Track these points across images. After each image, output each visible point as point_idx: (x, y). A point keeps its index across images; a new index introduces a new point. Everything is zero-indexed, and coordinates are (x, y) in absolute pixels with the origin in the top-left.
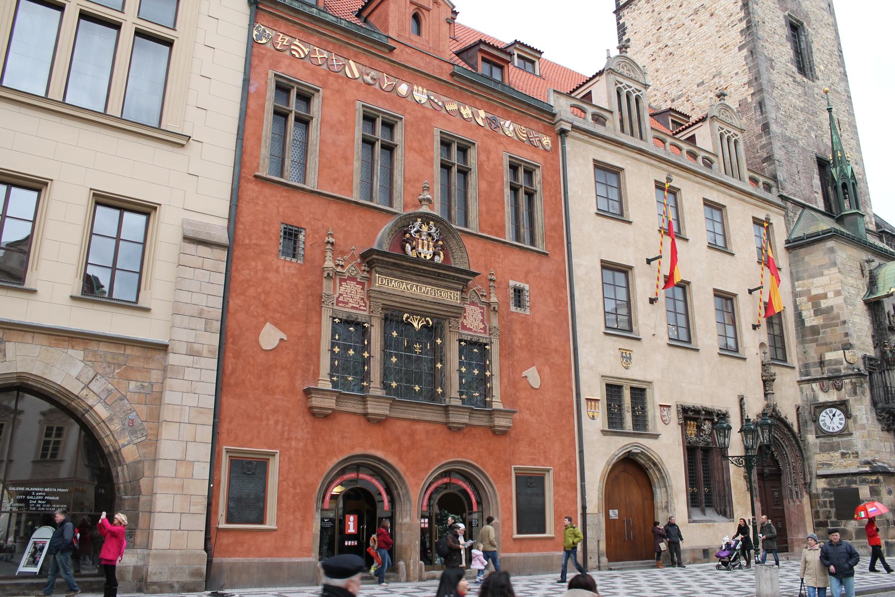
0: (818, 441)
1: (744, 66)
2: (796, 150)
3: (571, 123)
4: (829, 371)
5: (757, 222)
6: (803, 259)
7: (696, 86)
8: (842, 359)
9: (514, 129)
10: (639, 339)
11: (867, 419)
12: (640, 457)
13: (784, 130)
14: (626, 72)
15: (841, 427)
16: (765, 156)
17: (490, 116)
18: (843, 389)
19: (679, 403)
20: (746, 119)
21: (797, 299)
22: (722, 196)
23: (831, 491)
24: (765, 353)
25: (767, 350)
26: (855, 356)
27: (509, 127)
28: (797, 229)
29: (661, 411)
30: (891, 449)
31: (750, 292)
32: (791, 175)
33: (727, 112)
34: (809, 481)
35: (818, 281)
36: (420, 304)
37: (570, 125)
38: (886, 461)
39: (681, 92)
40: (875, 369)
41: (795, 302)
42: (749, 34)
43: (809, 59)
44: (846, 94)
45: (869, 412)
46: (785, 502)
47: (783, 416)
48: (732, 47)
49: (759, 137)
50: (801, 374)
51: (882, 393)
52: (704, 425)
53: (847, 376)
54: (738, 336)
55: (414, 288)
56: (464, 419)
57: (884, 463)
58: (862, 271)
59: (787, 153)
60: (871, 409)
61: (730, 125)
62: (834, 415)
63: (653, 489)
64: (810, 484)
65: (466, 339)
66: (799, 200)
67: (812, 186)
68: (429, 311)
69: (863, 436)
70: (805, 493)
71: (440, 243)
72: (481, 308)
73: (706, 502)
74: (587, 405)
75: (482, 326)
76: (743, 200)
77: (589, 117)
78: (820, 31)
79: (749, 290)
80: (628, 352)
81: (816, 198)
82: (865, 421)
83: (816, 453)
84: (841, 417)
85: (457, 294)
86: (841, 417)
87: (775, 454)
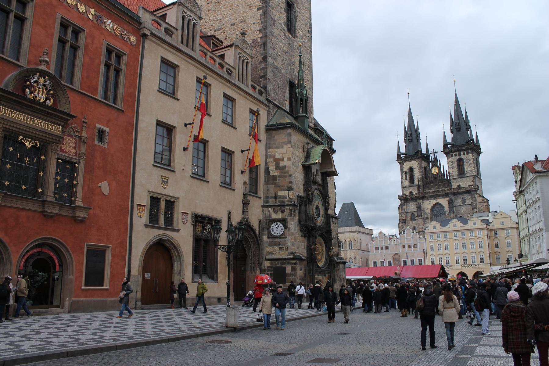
0: (268, 240)
1: (259, 20)
2: (279, 75)
3: (151, 31)
4: (279, 202)
5: (252, 112)
6: (274, 137)
7: (230, 25)
8: (286, 196)
9: (113, 27)
10: (174, 171)
11: (295, 230)
12: (167, 243)
13: (275, 62)
14: (190, 7)
15: (281, 233)
16: (262, 74)
17: (97, 14)
19: (193, 212)
20: (255, 51)
21: (268, 159)
22: (234, 93)
24: (246, 188)
25: (247, 186)
26: (293, 195)
27: (109, 24)
28: (273, 120)
29: (182, 216)
31: (242, 151)
32: (275, 88)
33: (245, 44)
34: (261, 262)
35: (280, 150)
36: (32, 131)
37: (150, 32)
38: (301, 253)
39: (221, 27)
40: (302, 203)
41: (266, 161)
42: (265, 2)
43: (294, 25)
44: (310, 49)
45: (296, 227)
46: (247, 273)
47: (251, 225)
48: (254, 7)
49: (260, 63)
50: (264, 202)
51: (304, 216)
52: (207, 226)
53: (288, 205)
54: (232, 176)
55: (29, 120)
56: (55, 210)
57: (300, 254)
58: (303, 148)
59: (274, 75)
60: (297, 224)
61: (245, 52)
62: (278, 226)
63: (173, 262)
64: (261, 264)
65: (62, 158)
66: (276, 103)
67: (285, 96)
68: (38, 136)
69: (292, 239)
70: (258, 268)
71: (52, 92)
72: (75, 139)
73: (203, 271)
74: (138, 208)
75: (74, 151)
76: (246, 98)
77: (163, 30)
78: (302, 11)
79: (242, 150)
80: (166, 178)
81: (285, 104)
82: (294, 231)
83: (266, 247)
84: (281, 228)
85: (59, 128)
86: (281, 228)
87: (245, 246)
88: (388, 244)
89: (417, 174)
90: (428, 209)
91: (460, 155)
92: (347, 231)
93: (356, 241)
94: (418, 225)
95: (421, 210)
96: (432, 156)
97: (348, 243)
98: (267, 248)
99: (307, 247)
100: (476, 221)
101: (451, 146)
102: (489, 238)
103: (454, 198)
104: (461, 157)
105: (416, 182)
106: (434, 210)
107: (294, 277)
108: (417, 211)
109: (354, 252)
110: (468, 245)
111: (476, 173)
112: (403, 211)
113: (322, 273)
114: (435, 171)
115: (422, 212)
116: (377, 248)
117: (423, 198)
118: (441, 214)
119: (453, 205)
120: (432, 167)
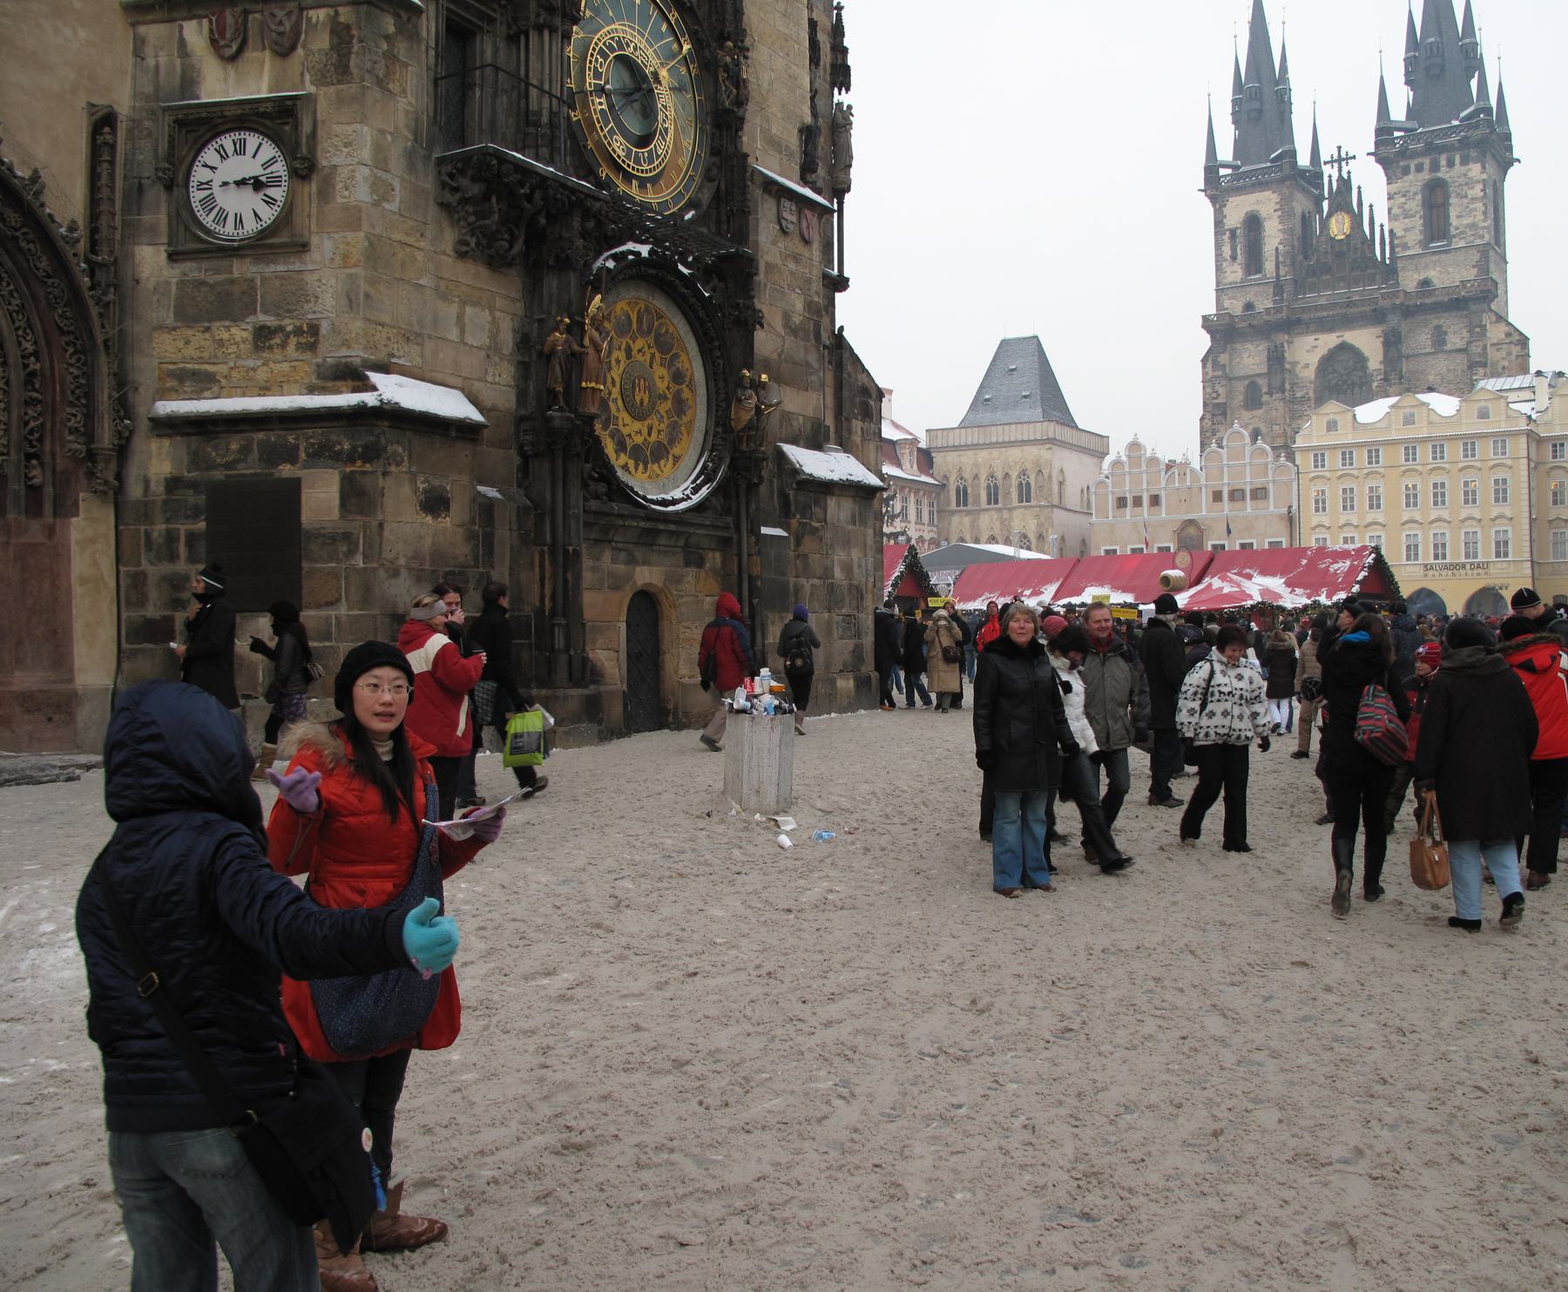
0: (173, 274)
11: (381, 191)
18: (300, 51)
23: (197, 492)
30: (494, 336)
34: (106, 437)
40: (491, 20)
45: (397, 163)
60: (410, 156)
69: (346, 257)
83: (161, 328)
88: (1161, 486)
89: (1273, 237)
90: (1307, 366)
91: (1435, 167)
92: (1013, 439)
93: (1046, 475)
94: (1271, 423)
95: (1283, 370)
96: (1329, 171)
97: (1014, 483)
98: (166, 337)
99: (524, 342)
100: (1489, 404)
101: (1402, 134)
102: (1534, 466)
103: (1404, 327)
104: (1440, 175)
105: (1269, 266)
106: (1330, 369)
107: (359, 561)
108: (1269, 373)
109: (1037, 516)
110: (1454, 492)
111: (1489, 233)
112: (1220, 373)
113: (662, 540)
114: (1339, 227)
115: (1287, 375)
116: (1121, 502)
117: (1293, 324)
118: (1354, 384)
119: (1399, 350)
120: (1330, 215)
